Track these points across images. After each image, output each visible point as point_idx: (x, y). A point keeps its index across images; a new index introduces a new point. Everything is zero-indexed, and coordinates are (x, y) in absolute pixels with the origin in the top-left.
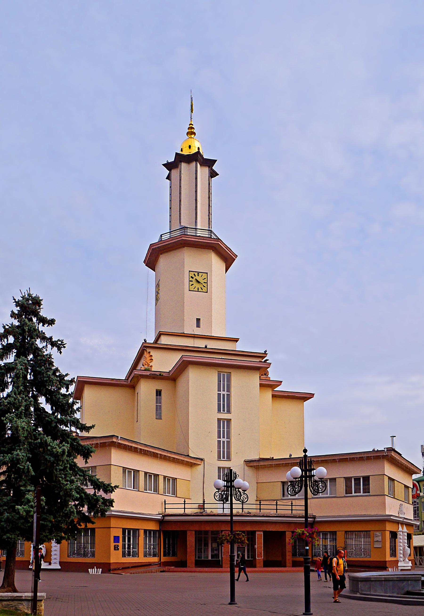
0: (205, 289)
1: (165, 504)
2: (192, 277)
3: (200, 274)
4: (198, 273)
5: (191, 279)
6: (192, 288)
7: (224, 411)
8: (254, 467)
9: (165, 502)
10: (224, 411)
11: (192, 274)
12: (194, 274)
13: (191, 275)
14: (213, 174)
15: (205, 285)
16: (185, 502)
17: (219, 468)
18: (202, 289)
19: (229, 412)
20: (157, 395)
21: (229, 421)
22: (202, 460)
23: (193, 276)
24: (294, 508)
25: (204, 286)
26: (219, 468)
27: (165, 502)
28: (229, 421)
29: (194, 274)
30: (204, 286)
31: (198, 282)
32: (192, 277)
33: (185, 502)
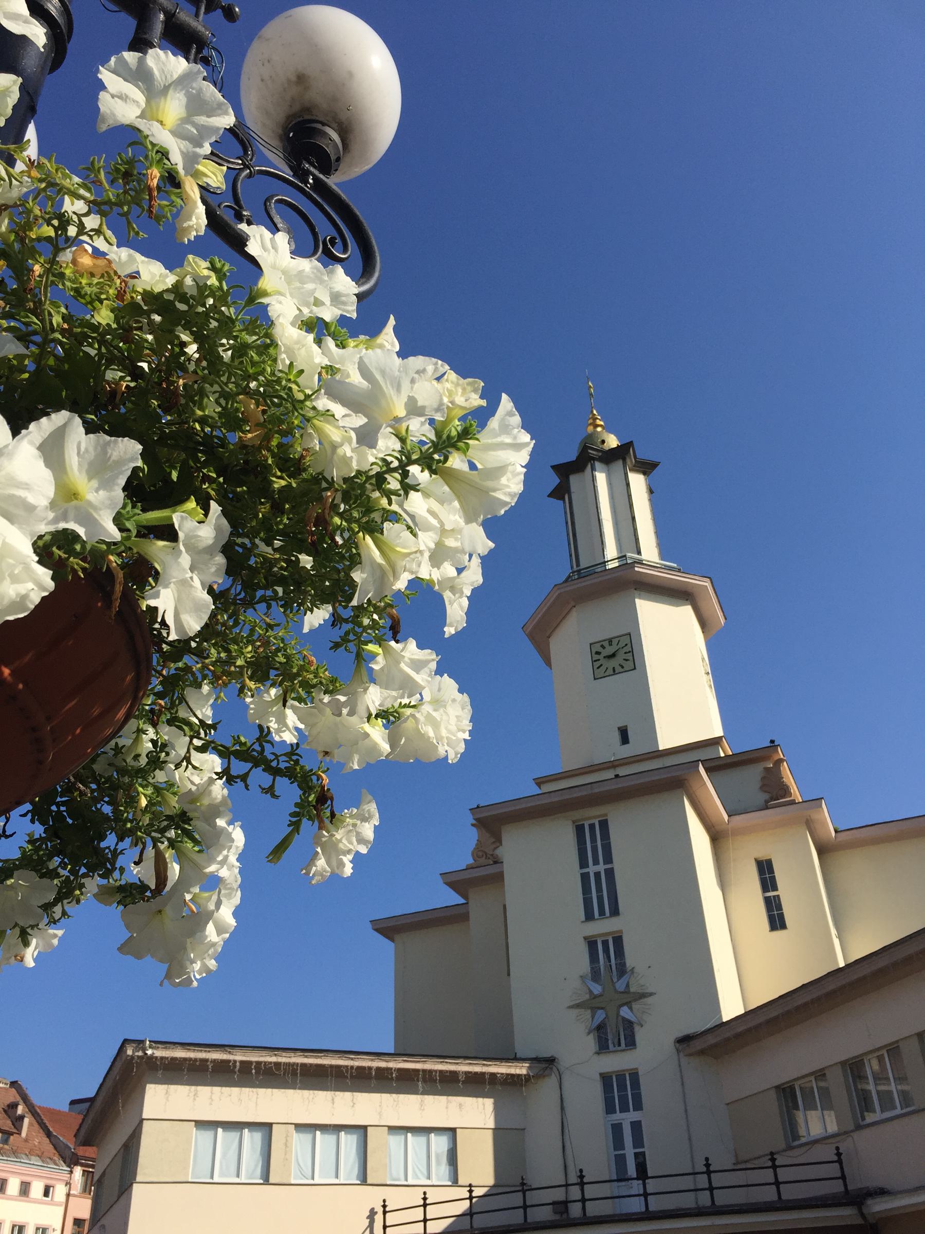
1: (385, 1213)
2: (598, 653)
4: (610, 641)
5: (596, 657)
7: (602, 912)
8: (702, 1052)
9: (384, 1206)
10: (602, 912)
11: (597, 648)
12: (603, 647)
13: (594, 651)
15: (629, 656)
16: (425, 1199)
17: (606, 1079)
18: (623, 667)
19: (615, 912)
23: (600, 649)
24: (783, 1174)
25: (627, 660)
26: (606, 1079)
27: (384, 1206)
29: (603, 647)
30: (627, 660)
31: (613, 655)
32: (598, 653)
33: (425, 1199)
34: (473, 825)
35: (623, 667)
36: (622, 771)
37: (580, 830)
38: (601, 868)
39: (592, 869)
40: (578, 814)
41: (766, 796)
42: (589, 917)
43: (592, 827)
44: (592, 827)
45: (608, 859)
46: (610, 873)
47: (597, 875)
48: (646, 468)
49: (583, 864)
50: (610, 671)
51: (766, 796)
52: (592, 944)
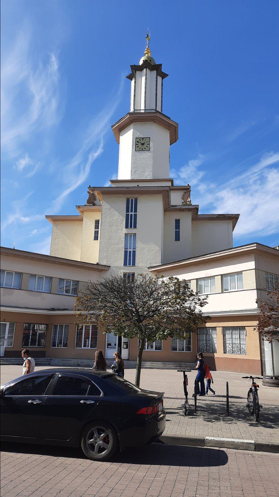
0: (147, 149)
3: (144, 139)
4: (143, 138)
5: (138, 143)
6: (137, 149)
11: (138, 140)
12: (140, 140)
14: (164, 76)
19: (135, 227)
20: (96, 223)
21: (135, 235)
22: (110, 267)
23: (139, 141)
25: (147, 147)
28: (135, 235)
29: (140, 140)
31: (143, 144)
34: (88, 192)
35: (145, 149)
36: (141, 185)
37: (128, 201)
38: (133, 213)
39: (130, 213)
40: (129, 196)
41: (183, 201)
42: (127, 227)
43: (132, 200)
44: (132, 200)
45: (136, 211)
46: (135, 215)
47: (131, 215)
48: (164, 76)
49: (127, 211)
50: (141, 149)
51: (183, 201)
52: (126, 235)
